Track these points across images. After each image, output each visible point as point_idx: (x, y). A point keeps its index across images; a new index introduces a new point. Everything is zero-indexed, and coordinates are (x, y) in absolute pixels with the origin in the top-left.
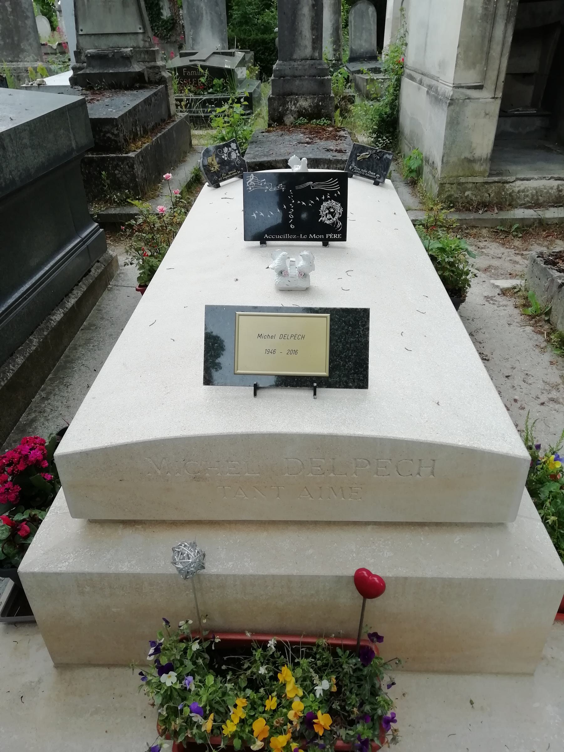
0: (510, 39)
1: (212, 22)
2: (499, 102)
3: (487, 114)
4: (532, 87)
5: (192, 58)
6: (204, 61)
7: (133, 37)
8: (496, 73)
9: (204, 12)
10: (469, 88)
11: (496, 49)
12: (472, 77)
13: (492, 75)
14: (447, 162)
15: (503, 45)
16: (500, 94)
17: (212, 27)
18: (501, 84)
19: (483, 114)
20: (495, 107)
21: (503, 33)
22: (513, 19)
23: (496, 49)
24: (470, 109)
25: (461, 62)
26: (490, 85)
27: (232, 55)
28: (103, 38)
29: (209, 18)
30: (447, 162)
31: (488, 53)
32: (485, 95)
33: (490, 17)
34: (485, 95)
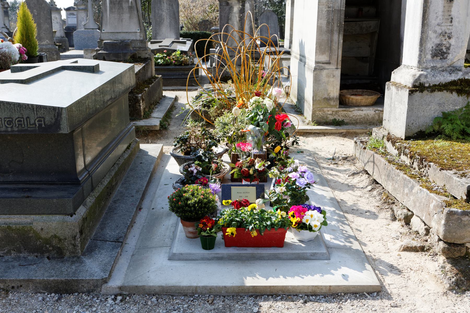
0: (342, 41)
1: (170, 23)
4: (368, 64)
5: (160, 44)
6: (168, 46)
7: (134, 34)
8: (336, 56)
9: (165, 18)
10: (323, 63)
12: (324, 58)
14: (316, 100)
15: (339, 43)
16: (340, 67)
17: (170, 26)
19: (332, 76)
21: (338, 39)
23: (335, 46)
24: (324, 73)
25: (318, 51)
26: (334, 61)
27: (184, 43)
28: (116, 34)
29: (168, 21)
30: (316, 100)
32: (332, 67)
33: (331, 32)
34: (332, 67)
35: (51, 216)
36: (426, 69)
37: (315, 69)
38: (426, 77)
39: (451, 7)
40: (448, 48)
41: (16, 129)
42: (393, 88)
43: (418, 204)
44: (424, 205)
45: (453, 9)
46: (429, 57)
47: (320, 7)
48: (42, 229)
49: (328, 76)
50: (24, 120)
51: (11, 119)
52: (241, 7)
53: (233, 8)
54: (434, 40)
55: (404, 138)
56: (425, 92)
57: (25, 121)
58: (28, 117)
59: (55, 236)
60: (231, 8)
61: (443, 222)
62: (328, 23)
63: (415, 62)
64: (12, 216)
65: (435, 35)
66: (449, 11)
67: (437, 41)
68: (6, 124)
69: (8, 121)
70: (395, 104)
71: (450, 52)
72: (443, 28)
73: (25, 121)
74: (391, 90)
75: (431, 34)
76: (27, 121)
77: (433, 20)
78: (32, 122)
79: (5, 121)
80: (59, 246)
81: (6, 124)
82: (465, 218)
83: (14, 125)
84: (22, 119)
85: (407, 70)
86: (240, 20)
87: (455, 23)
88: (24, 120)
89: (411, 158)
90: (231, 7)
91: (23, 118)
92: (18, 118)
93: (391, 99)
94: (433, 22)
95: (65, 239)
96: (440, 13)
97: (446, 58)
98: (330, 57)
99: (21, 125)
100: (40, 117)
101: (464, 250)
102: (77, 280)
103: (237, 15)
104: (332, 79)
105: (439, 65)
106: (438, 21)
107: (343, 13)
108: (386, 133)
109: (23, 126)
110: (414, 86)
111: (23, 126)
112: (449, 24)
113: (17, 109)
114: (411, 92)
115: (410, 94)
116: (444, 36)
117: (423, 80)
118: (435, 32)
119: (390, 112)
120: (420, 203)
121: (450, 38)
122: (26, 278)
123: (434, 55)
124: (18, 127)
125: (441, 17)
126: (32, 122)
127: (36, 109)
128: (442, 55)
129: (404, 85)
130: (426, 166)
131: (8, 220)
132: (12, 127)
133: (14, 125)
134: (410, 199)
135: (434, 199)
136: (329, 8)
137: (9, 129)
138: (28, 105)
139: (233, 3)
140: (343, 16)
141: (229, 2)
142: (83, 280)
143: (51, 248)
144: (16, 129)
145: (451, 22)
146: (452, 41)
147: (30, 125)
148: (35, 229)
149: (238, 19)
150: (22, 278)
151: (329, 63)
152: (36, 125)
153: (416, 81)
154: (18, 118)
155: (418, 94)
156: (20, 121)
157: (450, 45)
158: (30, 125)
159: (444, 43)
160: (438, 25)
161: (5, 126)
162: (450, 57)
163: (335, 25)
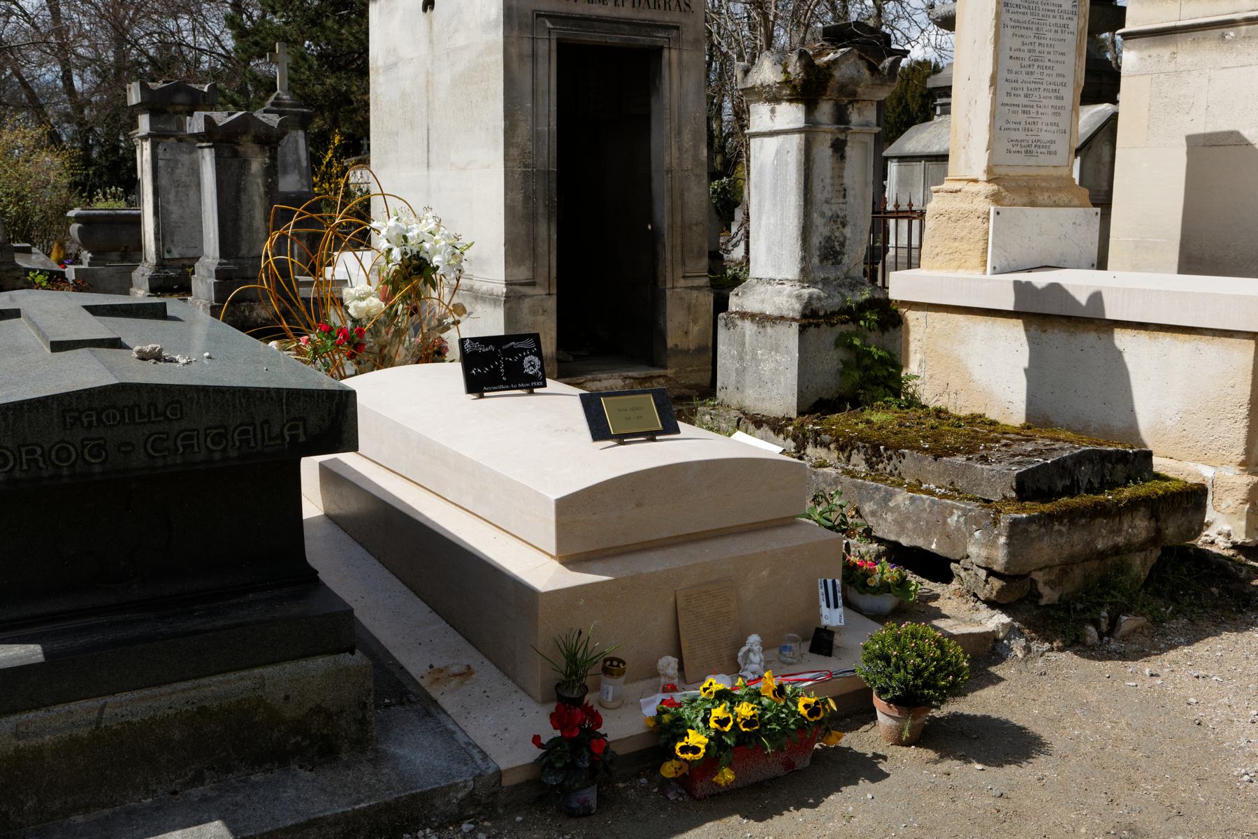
0: (555, 237)
2: (554, 298)
3: (545, 311)
11: (542, 248)
12: (523, 274)
13: (543, 272)
16: (554, 291)
18: (554, 281)
20: (552, 304)
21: (547, 233)
22: (554, 219)
23: (542, 248)
24: (526, 304)
31: (534, 250)
33: (532, 218)
34: (539, 291)
35: (303, 663)
36: (813, 283)
37: (508, 297)
38: (819, 298)
39: (842, 169)
40: (842, 245)
41: (233, 453)
42: (748, 327)
43: (910, 525)
44: (927, 523)
45: (846, 173)
46: (816, 260)
47: (509, 164)
48: (287, 698)
49: (534, 312)
50: (255, 429)
51: (222, 430)
52: (267, 160)
53: (250, 164)
54: (821, 229)
55: (794, 414)
56: (824, 326)
57: (259, 430)
58: (266, 422)
59: (318, 710)
60: (245, 164)
61: (1002, 540)
62: (526, 199)
63: (791, 269)
64: (204, 681)
65: (823, 221)
66: (841, 177)
67: (826, 231)
68: (209, 443)
69: (93, 446)
70: (754, 354)
71: (845, 250)
72: (834, 207)
73: (259, 431)
74: (738, 329)
75: (818, 220)
76: (263, 431)
77: (819, 196)
78: (276, 430)
79: (206, 436)
80: (325, 732)
81: (209, 443)
82: (1034, 527)
83: (231, 444)
84: (251, 428)
85: (769, 287)
86: (266, 193)
87: (850, 199)
88: (255, 429)
89: (841, 449)
90: (245, 161)
91: (253, 424)
92: (242, 424)
93: (743, 345)
94: (819, 196)
95: (342, 711)
96: (828, 181)
97: (839, 263)
98: (534, 270)
99: (248, 441)
100: (295, 419)
101: (1027, 587)
102: (423, 794)
103: (260, 181)
104: (541, 318)
105: (832, 277)
106: (826, 195)
107: (554, 176)
108: (734, 414)
109: (196, 449)
110: (804, 316)
111: (252, 444)
112: (842, 200)
113: (241, 404)
114: (803, 329)
115: (801, 332)
116: (835, 222)
117: (816, 304)
118: (823, 215)
119: (741, 372)
120: (916, 522)
121: (844, 225)
122: (302, 820)
123: (824, 258)
124: (239, 448)
125: (829, 188)
126: (276, 430)
127: (287, 400)
128: (835, 258)
129: (776, 313)
130: (890, 459)
131: (193, 693)
132: (224, 450)
133: (231, 444)
134: (886, 520)
135: (953, 507)
136: (526, 166)
137: (217, 456)
138: (268, 390)
139: (249, 151)
140: (554, 185)
141: (240, 148)
142: (434, 790)
143: (306, 743)
144: (233, 453)
145: (844, 196)
146: (848, 231)
147: (270, 439)
148: (269, 701)
149: (262, 189)
150: (290, 823)
151: (532, 284)
152: (284, 439)
153: (805, 308)
154: (242, 424)
155: (812, 330)
156: (246, 432)
157: (845, 238)
158: (270, 439)
159: (837, 234)
160: (827, 202)
161: (207, 448)
162: (846, 259)
163: (541, 203)
